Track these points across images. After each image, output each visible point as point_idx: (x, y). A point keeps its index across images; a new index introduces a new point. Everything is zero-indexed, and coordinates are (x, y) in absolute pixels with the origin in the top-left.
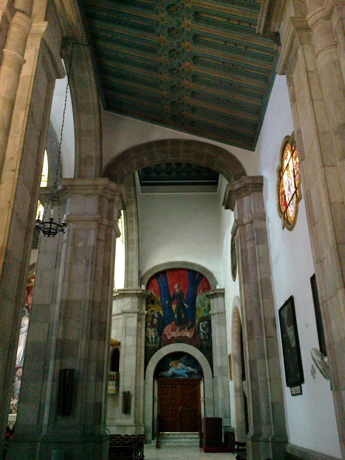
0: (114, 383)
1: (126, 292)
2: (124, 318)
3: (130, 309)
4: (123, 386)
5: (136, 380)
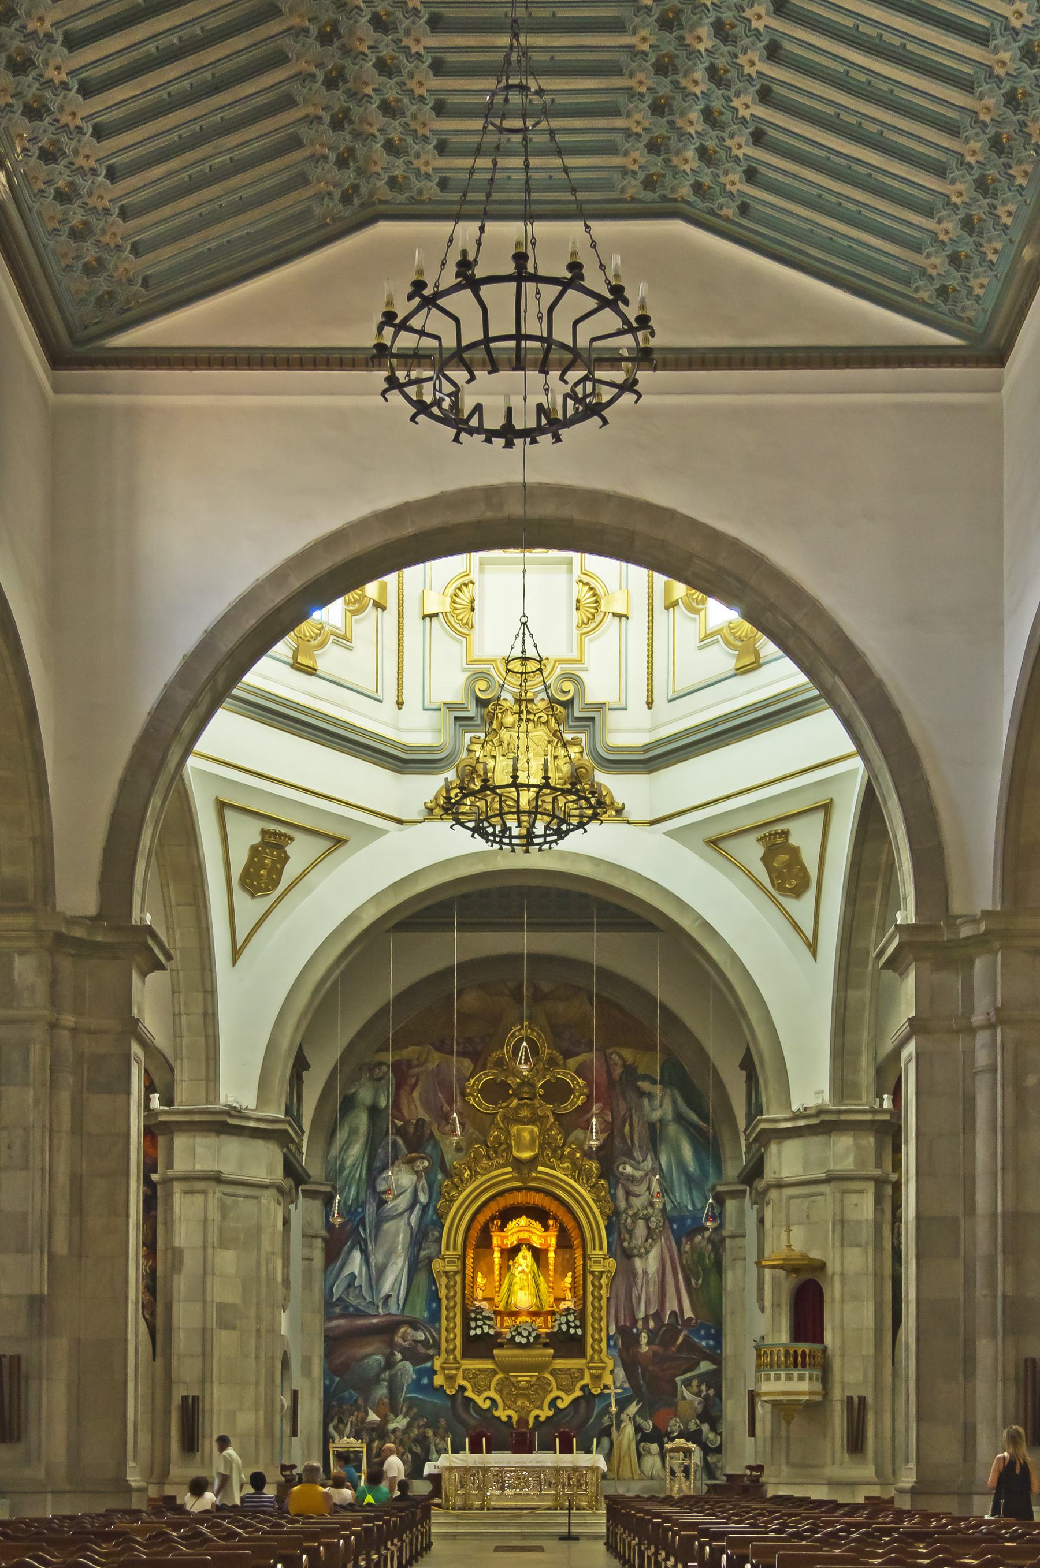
0: (816, 1373)
1: (843, 1117)
2: (838, 1195)
3: (852, 1167)
4: (842, 1383)
5: (878, 1368)
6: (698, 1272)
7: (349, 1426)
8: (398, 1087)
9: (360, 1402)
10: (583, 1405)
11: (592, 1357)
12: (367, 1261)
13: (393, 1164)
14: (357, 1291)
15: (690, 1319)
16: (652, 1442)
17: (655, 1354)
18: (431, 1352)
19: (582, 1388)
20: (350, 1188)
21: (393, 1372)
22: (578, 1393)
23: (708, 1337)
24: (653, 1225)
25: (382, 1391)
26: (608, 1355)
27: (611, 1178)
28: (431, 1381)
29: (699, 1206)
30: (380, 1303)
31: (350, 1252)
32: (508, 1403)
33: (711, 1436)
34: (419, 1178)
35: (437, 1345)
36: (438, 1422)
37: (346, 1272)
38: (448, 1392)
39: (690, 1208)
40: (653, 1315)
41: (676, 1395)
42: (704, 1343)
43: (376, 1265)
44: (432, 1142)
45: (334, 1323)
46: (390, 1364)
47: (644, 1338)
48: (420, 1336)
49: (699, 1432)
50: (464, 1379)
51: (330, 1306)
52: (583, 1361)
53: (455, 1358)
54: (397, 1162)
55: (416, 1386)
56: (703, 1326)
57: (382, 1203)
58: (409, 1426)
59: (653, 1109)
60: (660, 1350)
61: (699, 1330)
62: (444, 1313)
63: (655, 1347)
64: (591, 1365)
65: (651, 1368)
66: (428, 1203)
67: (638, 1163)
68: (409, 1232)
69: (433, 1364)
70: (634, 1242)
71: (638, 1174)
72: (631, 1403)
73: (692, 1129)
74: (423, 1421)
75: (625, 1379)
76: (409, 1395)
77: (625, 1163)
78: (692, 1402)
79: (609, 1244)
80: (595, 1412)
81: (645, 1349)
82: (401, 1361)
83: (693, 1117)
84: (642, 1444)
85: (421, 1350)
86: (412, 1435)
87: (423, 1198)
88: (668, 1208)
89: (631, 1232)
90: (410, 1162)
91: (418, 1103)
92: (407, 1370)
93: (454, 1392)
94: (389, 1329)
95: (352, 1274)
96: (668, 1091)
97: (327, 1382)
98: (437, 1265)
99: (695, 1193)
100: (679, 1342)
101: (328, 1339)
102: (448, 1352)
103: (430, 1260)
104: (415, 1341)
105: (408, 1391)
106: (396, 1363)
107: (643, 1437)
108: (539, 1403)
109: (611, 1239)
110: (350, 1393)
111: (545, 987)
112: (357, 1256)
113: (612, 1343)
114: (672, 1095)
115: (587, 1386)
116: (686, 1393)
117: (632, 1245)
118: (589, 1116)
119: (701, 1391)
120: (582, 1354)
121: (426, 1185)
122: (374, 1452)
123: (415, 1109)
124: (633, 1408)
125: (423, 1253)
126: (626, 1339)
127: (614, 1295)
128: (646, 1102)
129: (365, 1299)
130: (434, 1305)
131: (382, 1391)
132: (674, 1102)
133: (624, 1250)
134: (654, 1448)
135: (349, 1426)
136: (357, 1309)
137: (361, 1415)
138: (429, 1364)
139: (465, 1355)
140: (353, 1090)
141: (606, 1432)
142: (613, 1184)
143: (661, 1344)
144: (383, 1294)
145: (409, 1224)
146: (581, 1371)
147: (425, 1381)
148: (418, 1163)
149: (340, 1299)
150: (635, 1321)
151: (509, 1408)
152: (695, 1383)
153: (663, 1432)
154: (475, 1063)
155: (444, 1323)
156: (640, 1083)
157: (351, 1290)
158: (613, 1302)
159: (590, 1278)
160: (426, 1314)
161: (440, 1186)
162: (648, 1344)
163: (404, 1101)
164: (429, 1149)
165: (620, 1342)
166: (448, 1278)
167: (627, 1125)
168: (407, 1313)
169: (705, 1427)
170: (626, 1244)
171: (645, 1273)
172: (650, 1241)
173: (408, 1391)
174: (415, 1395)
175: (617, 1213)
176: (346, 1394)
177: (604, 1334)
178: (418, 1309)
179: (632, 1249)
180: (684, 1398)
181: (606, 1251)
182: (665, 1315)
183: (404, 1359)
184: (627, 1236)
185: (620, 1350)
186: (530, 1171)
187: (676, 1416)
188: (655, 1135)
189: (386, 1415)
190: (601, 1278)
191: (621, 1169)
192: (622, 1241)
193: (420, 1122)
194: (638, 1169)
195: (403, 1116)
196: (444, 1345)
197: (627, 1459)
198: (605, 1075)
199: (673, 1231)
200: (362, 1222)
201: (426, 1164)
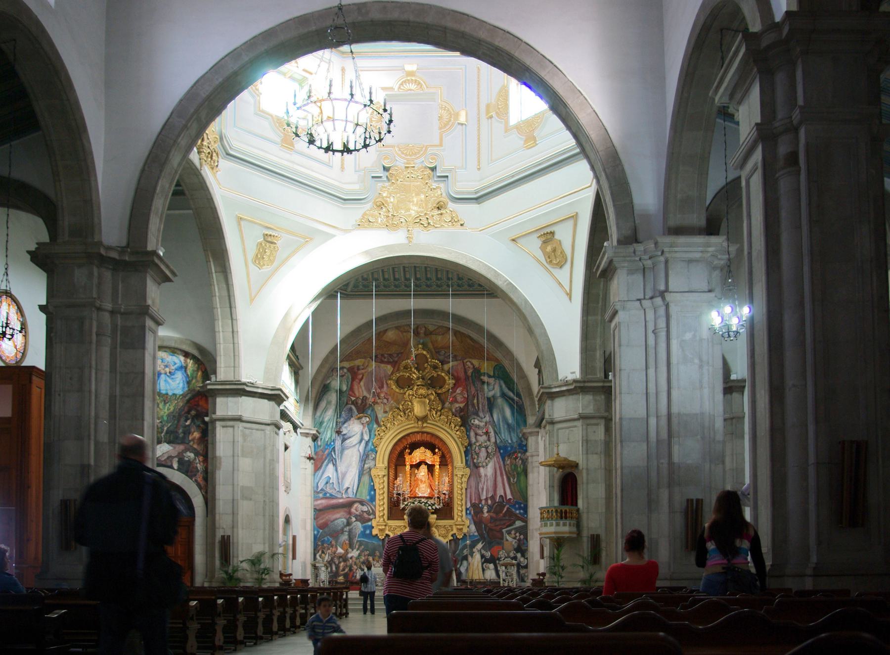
6: (514, 475)
7: (327, 555)
8: (353, 380)
9: (333, 542)
10: (453, 543)
12: (336, 470)
13: (350, 419)
14: (331, 485)
15: (510, 499)
16: (490, 563)
17: (491, 517)
18: (371, 517)
19: (452, 536)
20: (326, 434)
21: (351, 527)
23: (520, 508)
24: (490, 451)
25: (344, 537)
26: (467, 518)
27: (467, 426)
28: (371, 532)
29: (514, 440)
30: (344, 492)
31: (327, 465)
33: (522, 559)
34: (364, 428)
35: (374, 513)
37: (325, 476)
38: (380, 537)
39: (510, 441)
41: (502, 539)
42: (518, 512)
43: (341, 472)
44: (371, 408)
45: (319, 502)
46: (349, 524)
47: (485, 509)
50: (389, 531)
51: (317, 493)
52: (452, 521)
53: (384, 520)
54: (352, 419)
55: (363, 534)
56: (516, 503)
57: (344, 440)
58: (360, 555)
59: (489, 391)
60: (494, 515)
61: (515, 505)
62: (377, 497)
63: (492, 514)
64: (457, 523)
66: (369, 440)
67: (482, 418)
68: (359, 454)
70: (480, 459)
71: (482, 424)
72: (479, 543)
73: (510, 401)
75: (475, 530)
77: (474, 419)
78: (512, 542)
79: (467, 461)
80: (460, 548)
81: (486, 515)
83: (511, 394)
85: (366, 515)
86: (361, 560)
87: (366, 438)
88: (498, 442)
89: (478, 454)
90: (359, 418)
91: (363, 388)
92: (358, 527)
93: (383, 537)
94: (349, 505)
95: (329, 476)
96: (497, 381)
97: (316, 532)
98: (373, 472)
99: (512, 434)
100: (504, 512)
103: (370, 469)
106: (352, 523)
107: (485, 560)
109: (467, 458)
110: (328, 538)
111: (431, 328)
112: (331, 466)
113: (468, 512)
114: (500, 383)
115: (455, 534)
116: (508, 537)
117: (479, 461)
118: (455, 394)
119: (516, 536)
120: (453, 519)
121: (368, 431)
122: (341, 568)
123: (361, 391)
125: (366, 466)
126: (475, 510)
127: (469, 487)
128: (486, 387)
130: (372, 493)
131: (344, 537)
132: (501, 387)
133: (474, 464)
134: (492, 566)
135: (327, 555)
136: (331, 495)
138: (370, 523)
139: (388, 519)
140: (328, 382)
141: (465, 558)
142: (468, 431)
143: (494, 512)
144: (345, 487)
145: (359, 451)
146: (451, 526)
147: (368, 532)
148: (364, 419)
149: (322, 490)
150: (481, 501)
152: (513, 532)
153: (496, 557)
154: (394, 367)
156: (482, 377)
157: (328, 485)
158: (468, 491)
160: (368, 498)
161: (375, 431)
162: (487, 512)
163: (356, 387)
164: (369, 412)
165: (472, 512)
167: (476, 398)
169: (519, 555)
170: (475, 461)
171: (486, 476)
172: (488, 459)
174: (362, 539)
175: (470, 444)
176: (326, 538)
177: (464, 507)
178: (364, 495)
179: (479, 463)
180: (507, 540)
181: (464, 463)
184: (476, 457)
185: (472, 516)
186: (423, 423)
188: (491, 404)
189: (347, 549)
190: (462, 478)
191: (472, 422)
192: (473, 459)
193: (365, 399)
194: (481, 422)
195: (355, 394)
197: (477, 572)
198: (463, 374)
199: (501, 453)
200: (334, 449)
201: (368, 419)
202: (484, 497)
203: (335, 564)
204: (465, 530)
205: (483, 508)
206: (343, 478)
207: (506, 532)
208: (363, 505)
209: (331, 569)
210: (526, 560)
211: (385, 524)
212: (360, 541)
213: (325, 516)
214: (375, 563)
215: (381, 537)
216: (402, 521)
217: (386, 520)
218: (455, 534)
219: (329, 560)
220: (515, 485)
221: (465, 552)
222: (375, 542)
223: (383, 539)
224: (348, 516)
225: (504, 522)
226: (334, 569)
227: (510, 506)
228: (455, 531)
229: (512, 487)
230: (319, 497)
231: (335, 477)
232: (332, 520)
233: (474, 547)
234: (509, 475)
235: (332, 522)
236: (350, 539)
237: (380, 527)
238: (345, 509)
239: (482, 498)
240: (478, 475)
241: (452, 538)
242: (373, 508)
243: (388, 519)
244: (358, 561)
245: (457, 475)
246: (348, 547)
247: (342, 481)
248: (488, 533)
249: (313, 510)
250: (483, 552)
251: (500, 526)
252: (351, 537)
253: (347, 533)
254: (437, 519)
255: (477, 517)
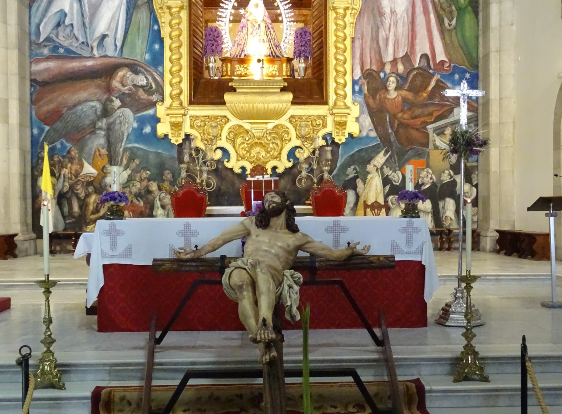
6: (451, 12)
11: (335, 104)
14: (68, 30)
15: (443, 62)
17: (404, 100)
18: (154, 98)
19: (324, 138)
21: (111, 120)
22: (321, 142)
28: (154, 130)
30: (95, 44)
32: (242, 152)
33: (467, 187)
35: (160, 90)
36: (162, 174)
37: (54, 9)
40: (402, 58)
41: (427, 145)
45: (43, 66)
46: (106, 112)
47: (392, 83)
48: (141, 80)
49: (453, 183)
52: (326, 107)
53: (181, 104)
55: (139, 135)
56: (455, 70)
58: (130, 179)
61: (452, 74)
62: (167, 54)
63: (404, 93)
64: (335, 111)
65: (400, 115)
69: (156, 111)
72: (378, 153)
74: (146, 174)
75: (372, 127)
76: (130, 145)
80: (338, 165)
81: (393, 94)
82: (118, 108)
84: (391, 197)
85: (142, 94)
86: (134, 190)
93: (180, 141)
95: (62, 11)
97: (35, 131)
100: (430, 88)
101: (33, 82)
102: (171, 97)
104: (135, 86)
105: (129, 140)
108: (276, 153)
110: (62, 144)
113: (357, 88)
115: (331, 134)
120: (326, 103)
122: (91, 208)
124: (380, 159)
127: (360, 36)
129: (77, 39)
130: (157, 46)
136: (68, 50)
137: (75, 167)
138: (151, 112)
139: (191, 103)
141: (352, 184)
143: (409, 90)
146: (323, 118)
147: (148, 129)
149: (48, 39)
150: (383, 64)
151: (242, 159)
155: (167, 64)
157: (61, 29)
158: (358, 43)
159: (331, 15)
160: (147, 57)
162: (396, 89)
166: (171, 14)
168: (126, 53)
169: (460, 179)
171: (393, 12)
173: (129, 140)
174: (136, 145)
177: (348, 78)
178: (138, 50)
180: (436, 148)
182: (415, 61)
183: (124, 105)
187: (428, 166)
189: (104, 167)
190: (345, 16)
196: (167, 90)
202: (388, 57)
203: (78, 198)
204: (353, 128)
205: (387, 80)
206: (93, 15)
207: (435, 130)
208: (136, 72)
209: (71, 207)
210: (475, 190)
211: (182, 112)
212: (131, 149)
213: (55, 94)
214: (163, 195)
215: (177, 140)
216: (221, 107)
217: (185, 103)
218: (331, 134)
219: (66, 189)
220: (453, 33)
221: (351, 172)
222: (165, 153)
223: (180, 145)
224: (105, 97)
225: (431, 109)
226: (76, 208)
227: (443, 76)
228: (330, 128)
229: (447, 37)
230: (42, 54)
231: (75, 12)
232: (70, 103)
233: (369, 162)
234: (442, 12)
235: (70, 108)
236: (110, 145)
237: (173, 120)
238: (98, 81)
239: (384, 60)
240: (376, 12)
241: (323, 143)
242: (158, 78)
243: (191, 103)
244: (127, 190)
245: (334, 9)
246: (106, 160)
247: (91, 22)
248: (396, 132)
249: (28, 83)
250: (387, 171)
251: (422, 119)
252: (113, 140)
253: (103, 133)
254: (293, 103)
255: (374, 98)
